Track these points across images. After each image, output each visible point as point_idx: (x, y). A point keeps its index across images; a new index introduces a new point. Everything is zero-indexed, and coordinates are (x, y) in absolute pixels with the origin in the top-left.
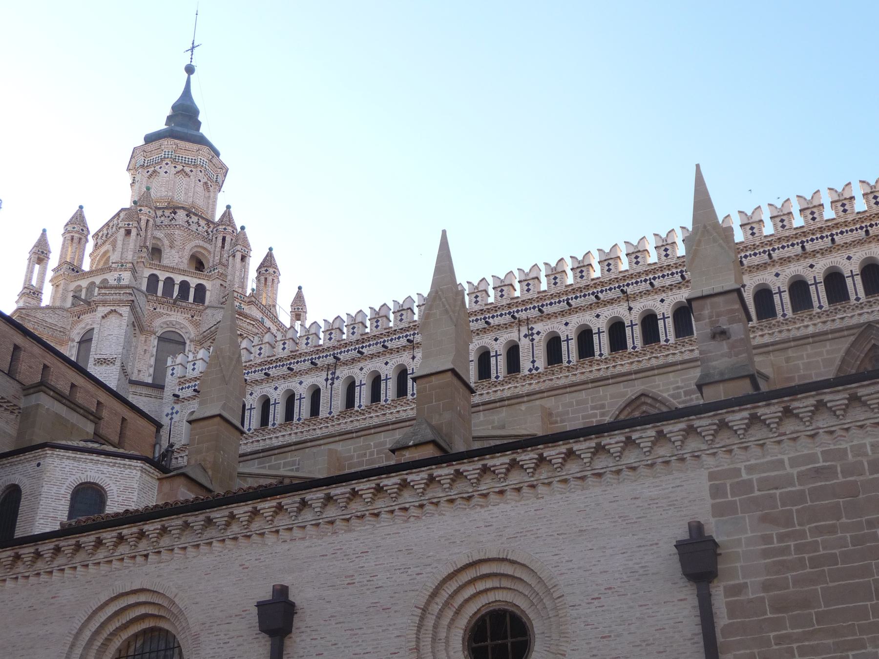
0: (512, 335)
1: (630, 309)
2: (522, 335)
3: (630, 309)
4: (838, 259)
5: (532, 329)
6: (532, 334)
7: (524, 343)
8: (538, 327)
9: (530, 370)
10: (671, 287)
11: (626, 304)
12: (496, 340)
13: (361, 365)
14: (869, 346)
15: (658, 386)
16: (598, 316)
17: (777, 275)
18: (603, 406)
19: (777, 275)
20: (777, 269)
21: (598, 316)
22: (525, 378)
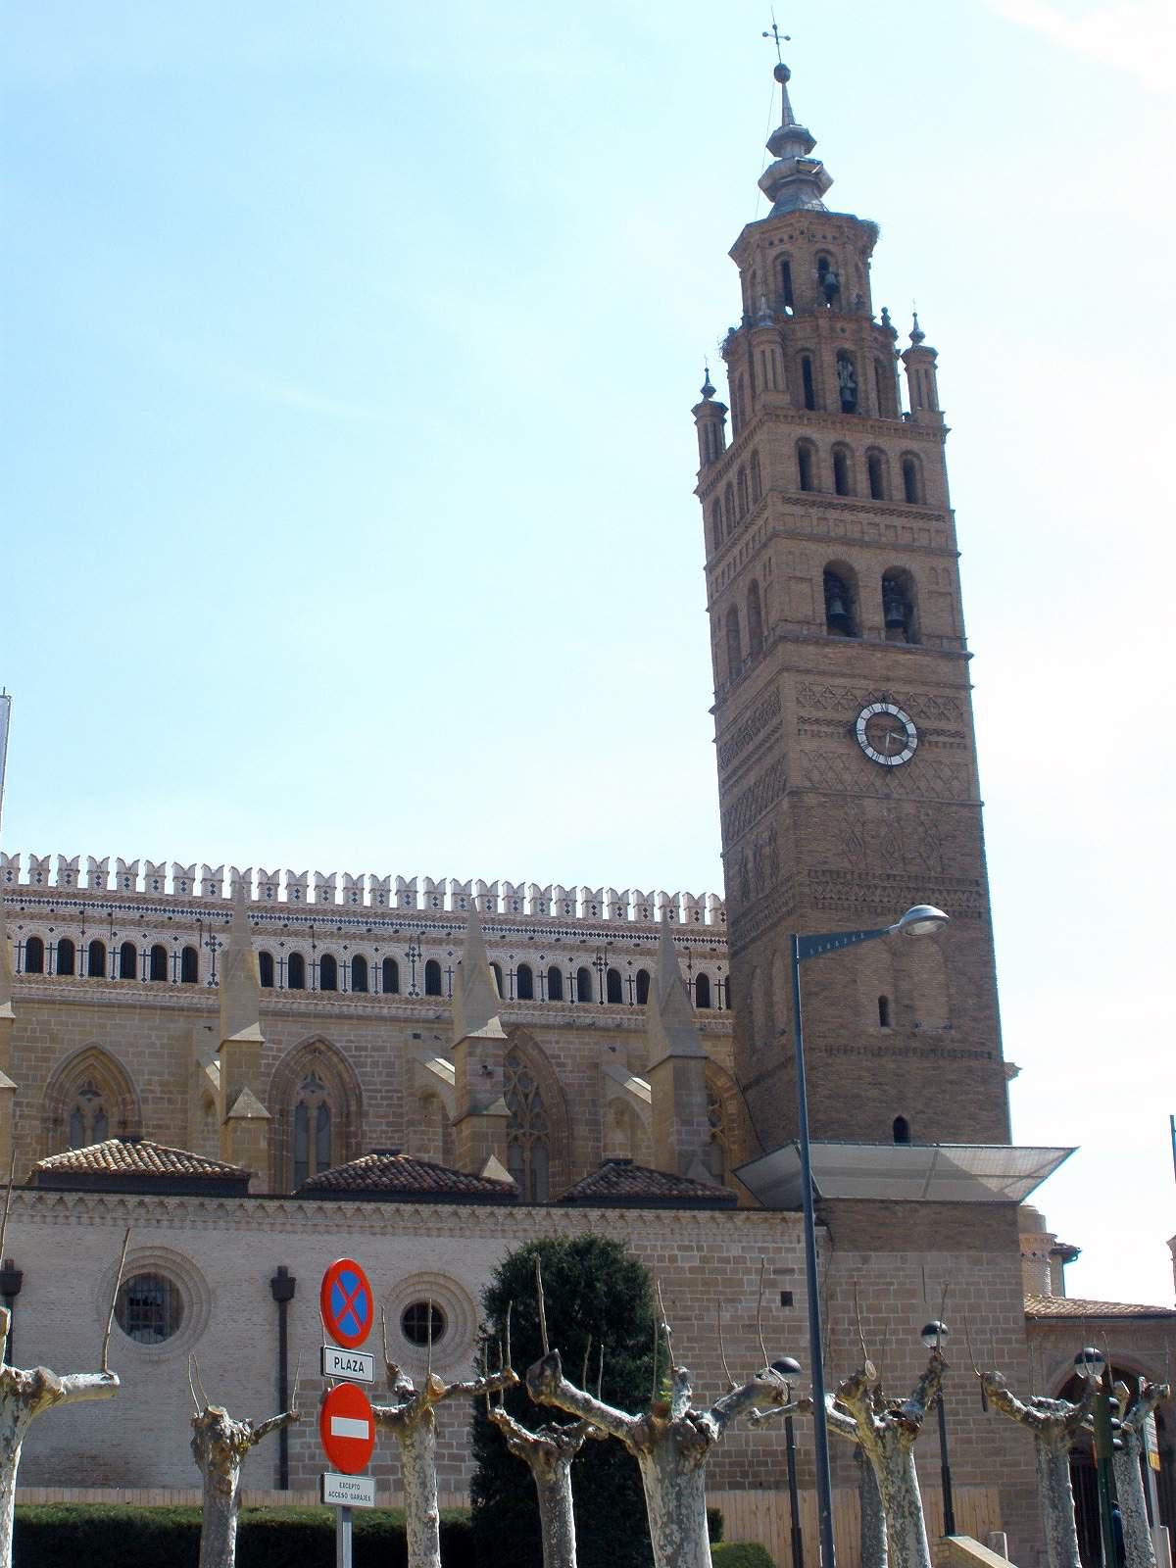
0: (192, 939)
1: (314, 947)
2: (204, 941)
3: (314, 947)
4: (502, 955)
5: (214, 938)
6: (214, 944)
7: (204, 953)
8: (221, 938)
9: (210, 983)
10: (354, 937)
11: (311, 940)
12: (176, 939)
13: (21, 923)
14: (513, 1045)
15: (333, 1035)
16: (282, 944)
17: (450, 954)
18: (279, 1042)
19: (450, 954)
20: (451, 948)
21: (282, 944)
22: (202, 991)
